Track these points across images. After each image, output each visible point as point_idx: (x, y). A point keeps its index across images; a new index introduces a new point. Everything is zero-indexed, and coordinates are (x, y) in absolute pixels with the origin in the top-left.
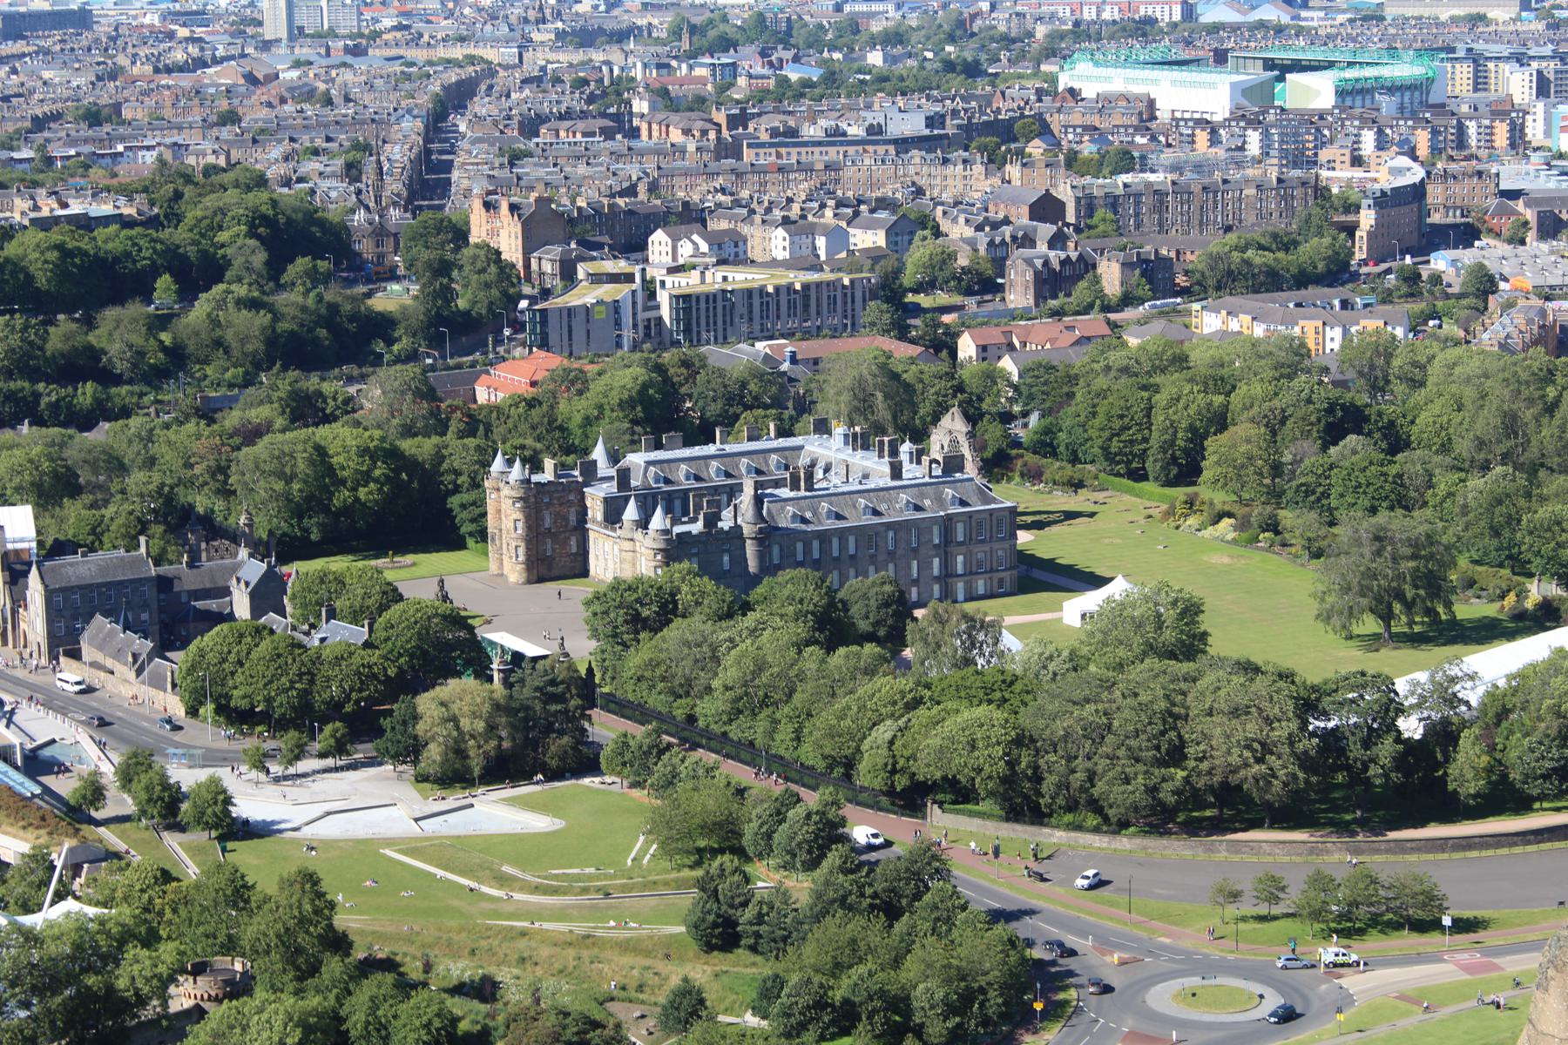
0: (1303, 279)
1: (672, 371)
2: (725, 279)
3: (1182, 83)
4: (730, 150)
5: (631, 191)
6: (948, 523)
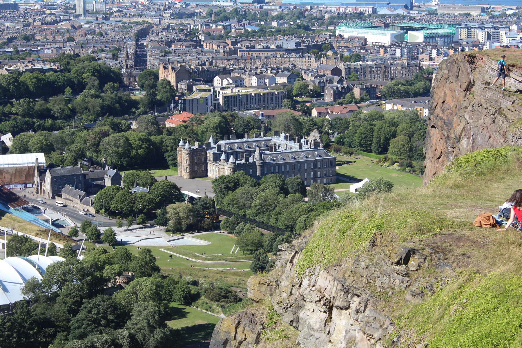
0: (416, 94)
1: (228, 118)
2: (239, 91)
3: (376, 34)
4: (233, 52)
5: (204, 64)
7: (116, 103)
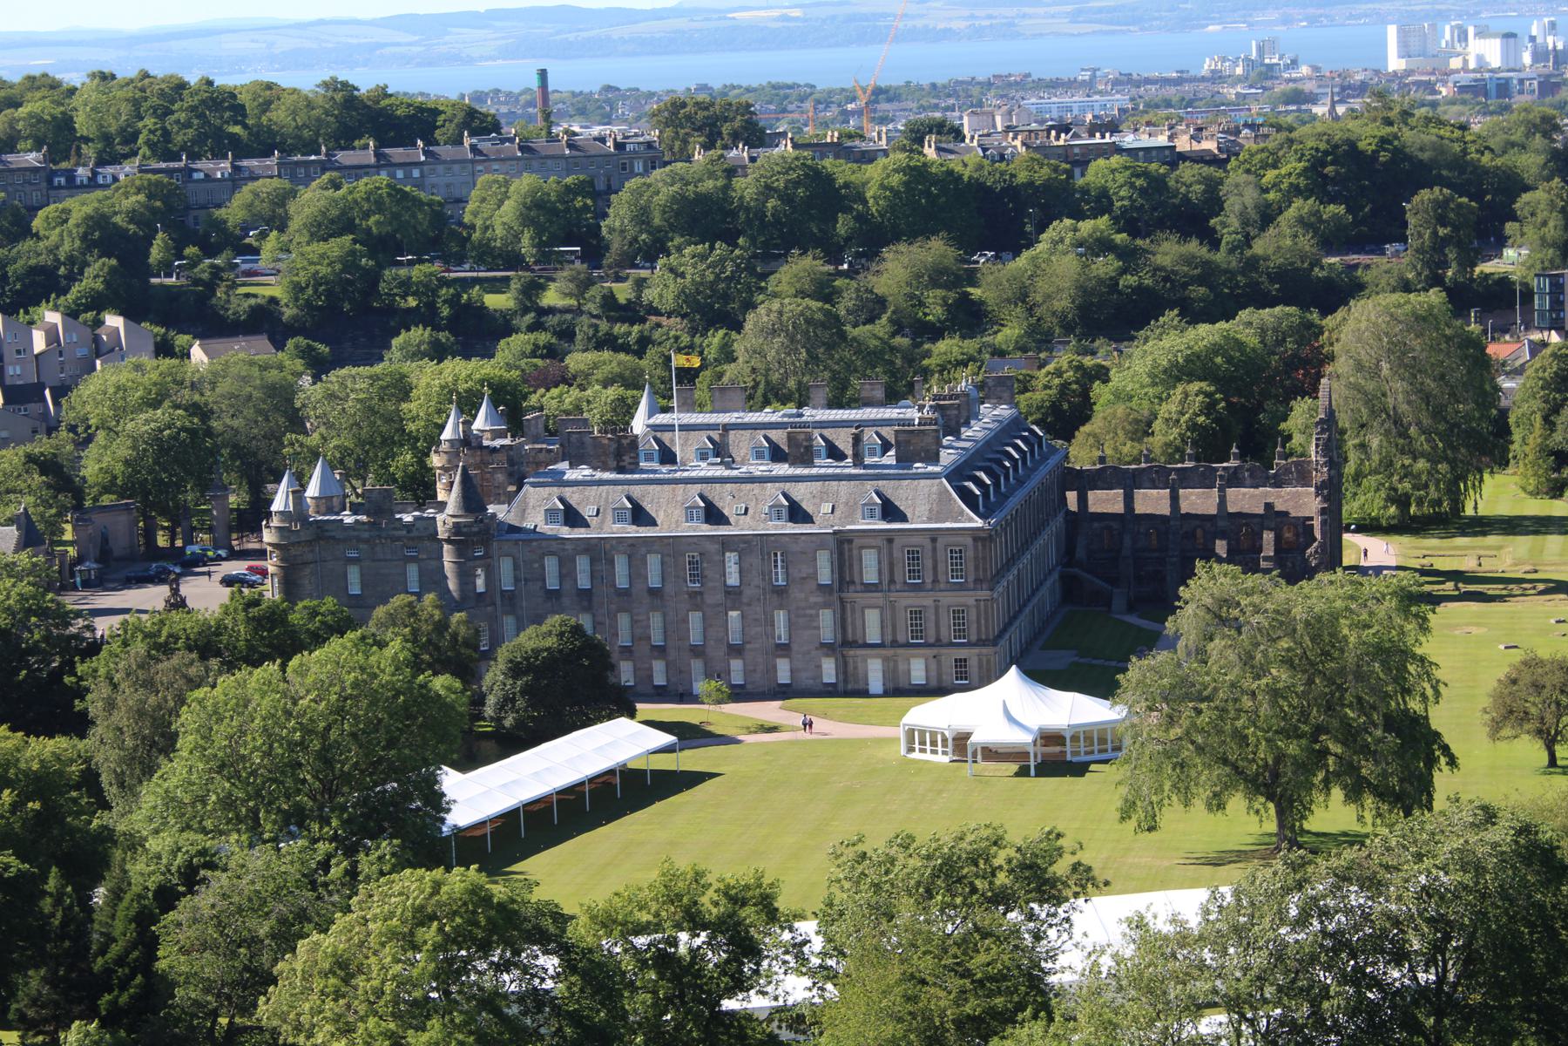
7: (1200, 280)
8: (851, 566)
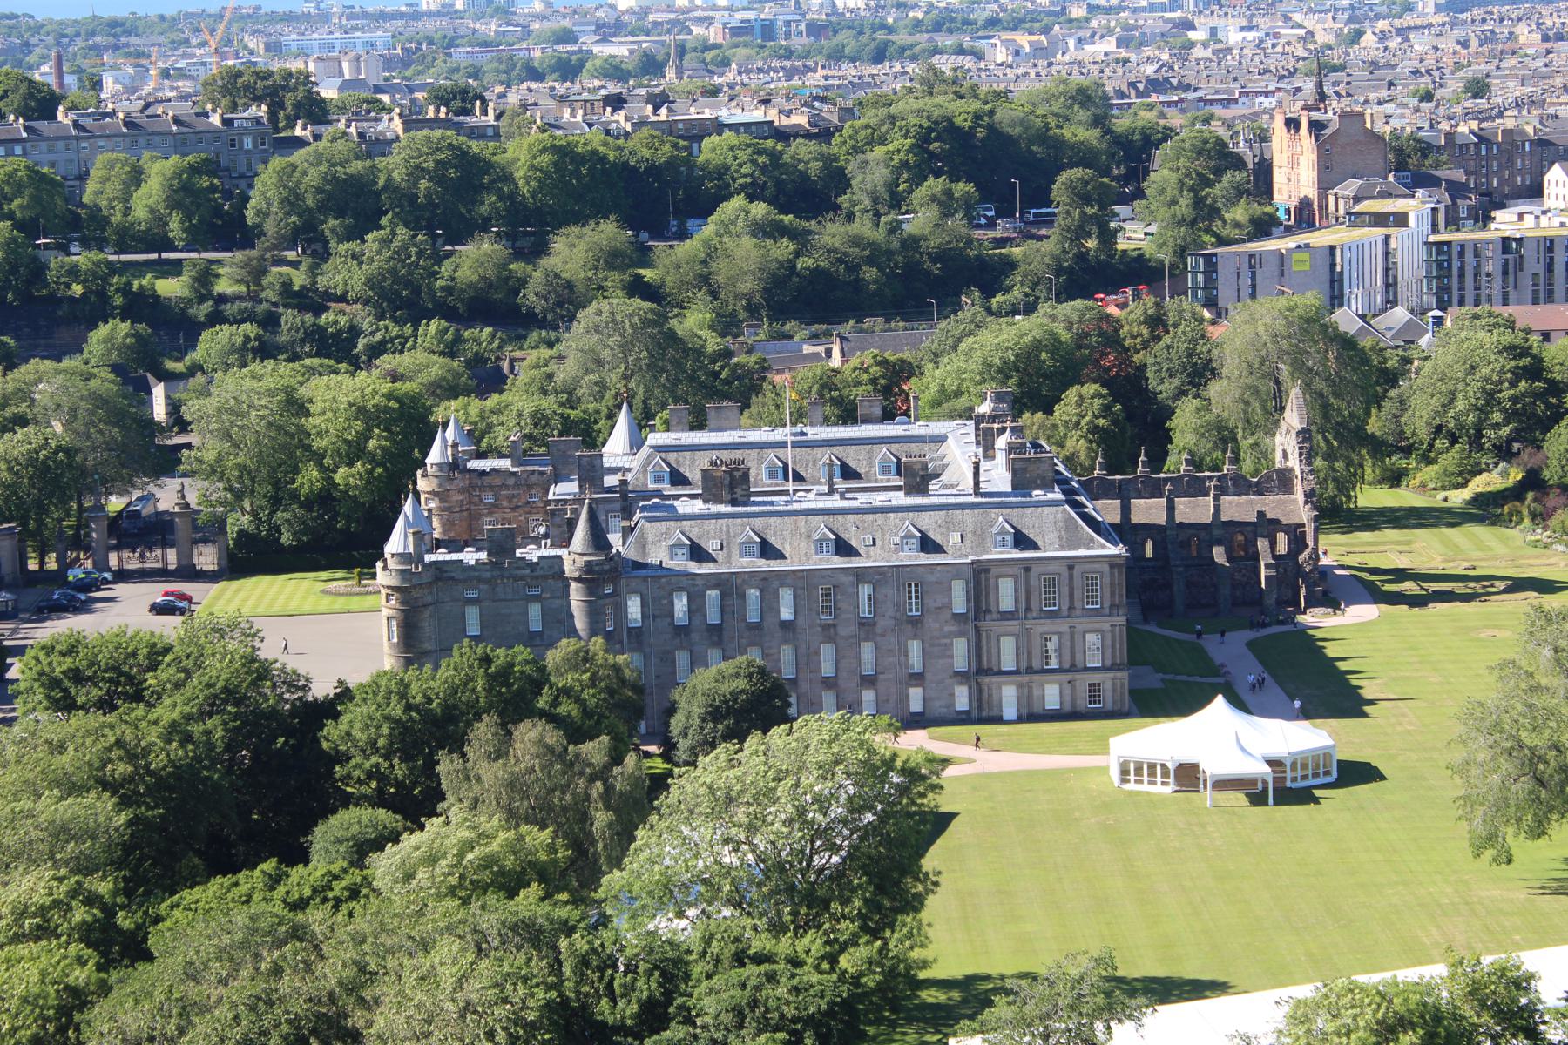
1: (1124, 331)
6: (980, 576)
7: (871, 261)
8: (988, 594)
